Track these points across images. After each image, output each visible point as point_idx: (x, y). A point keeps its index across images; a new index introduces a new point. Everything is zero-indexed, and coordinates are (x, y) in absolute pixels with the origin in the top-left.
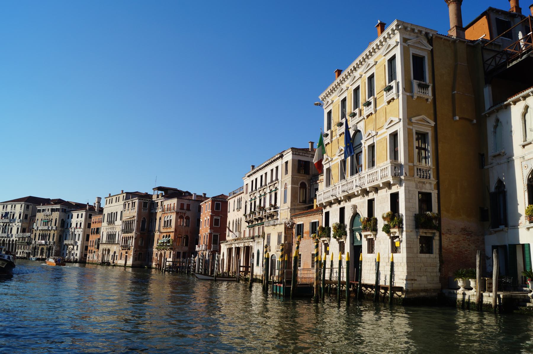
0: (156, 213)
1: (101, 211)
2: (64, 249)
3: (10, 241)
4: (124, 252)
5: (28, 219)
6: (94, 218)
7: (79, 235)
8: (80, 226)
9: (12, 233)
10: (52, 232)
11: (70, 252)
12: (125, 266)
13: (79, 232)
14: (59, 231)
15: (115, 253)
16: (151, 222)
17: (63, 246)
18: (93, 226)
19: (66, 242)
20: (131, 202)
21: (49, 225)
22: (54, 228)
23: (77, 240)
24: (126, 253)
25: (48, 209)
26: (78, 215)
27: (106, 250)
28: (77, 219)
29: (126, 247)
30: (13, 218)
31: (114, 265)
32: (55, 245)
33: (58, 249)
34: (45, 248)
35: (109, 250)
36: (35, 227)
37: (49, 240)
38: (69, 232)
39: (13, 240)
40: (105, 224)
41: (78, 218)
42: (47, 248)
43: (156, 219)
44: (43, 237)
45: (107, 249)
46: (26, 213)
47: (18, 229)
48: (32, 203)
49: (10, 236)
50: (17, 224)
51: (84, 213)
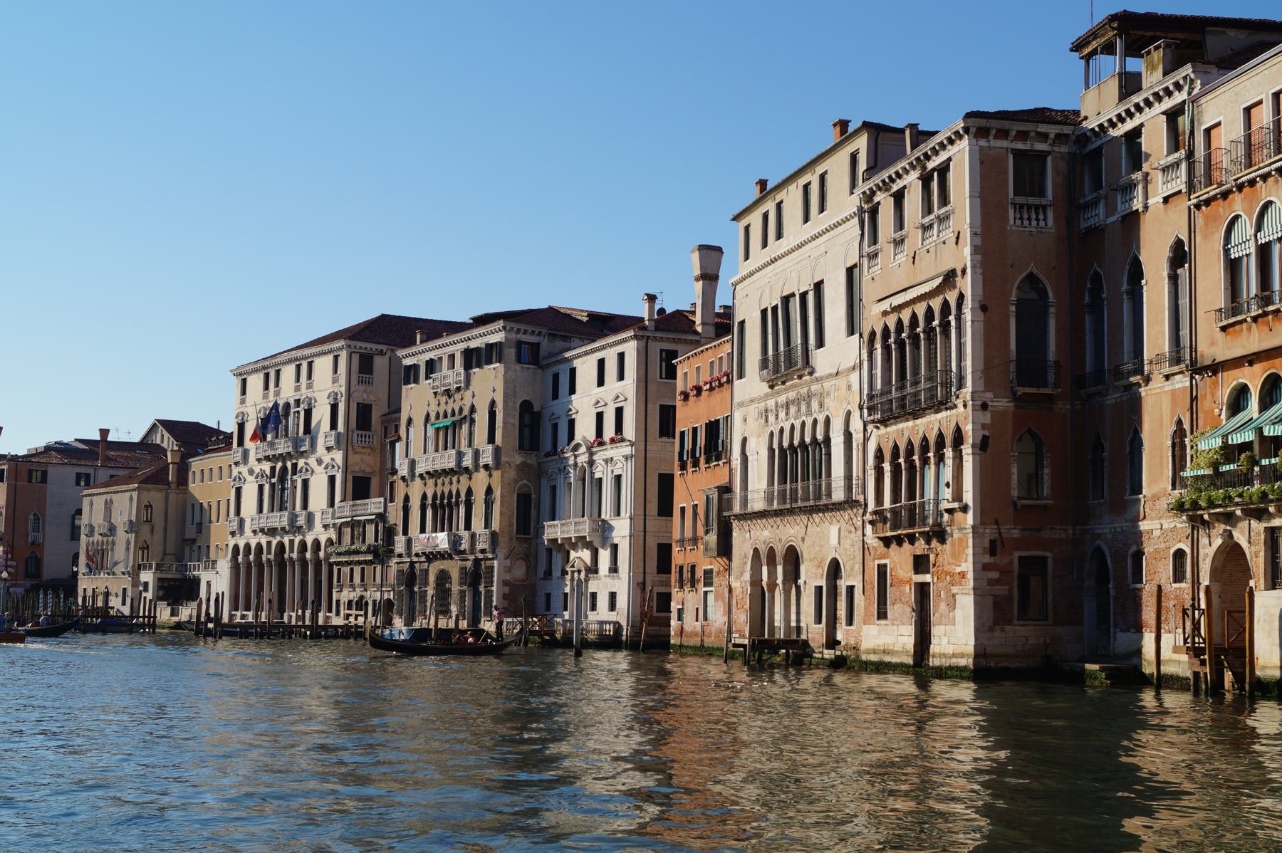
0: (1132, 220)
1: (723, 324)
2: (549, 573)
3: (303, 545)
4: (900, 560)
5: (371, 423)
6: (690, 369)
7: (618, 478)
8: (619, 427)
9: (311, 508)
10: (480, 482)
11: (580, 586)
12: (921, 667)
13: (616, 462)
14: (512, 474)
15: (835, 570)
16: (1096, 308)
17: (543, 556)
18: (690, 417)
19: (554, 531)
20: (912, 180)
21: (464, 442)
22: (487, 458)
23: (607, 513)
24: (921, 564)
25: (452, 357)
26: (601, 363)
27: (771, 552)
28: (601, 390)
29: (908, 523)
30: (307, 430)
31: (839, 664)
32: (501, 552)
33: (519, 572)
34: (455, 575)
35: (793, 559)
36: (402, 468)
37: (468, 526)
38: (563, 470)
39: (317, 543)
40: (751, 385)
41: (601, 382)
42: (463, 570)
43: (1137, 273)
44: (442, 511)
45: (780, 551)
46: (361, 395)
47: (332, 479)
48: (381, 343)
49: (301, 521)
50: (327, 459)
51: (631, 350)
